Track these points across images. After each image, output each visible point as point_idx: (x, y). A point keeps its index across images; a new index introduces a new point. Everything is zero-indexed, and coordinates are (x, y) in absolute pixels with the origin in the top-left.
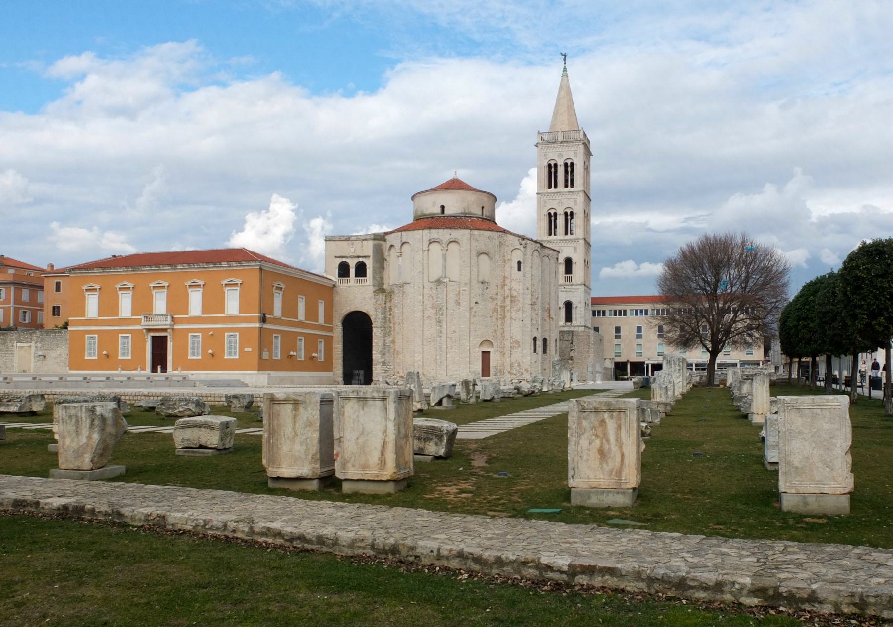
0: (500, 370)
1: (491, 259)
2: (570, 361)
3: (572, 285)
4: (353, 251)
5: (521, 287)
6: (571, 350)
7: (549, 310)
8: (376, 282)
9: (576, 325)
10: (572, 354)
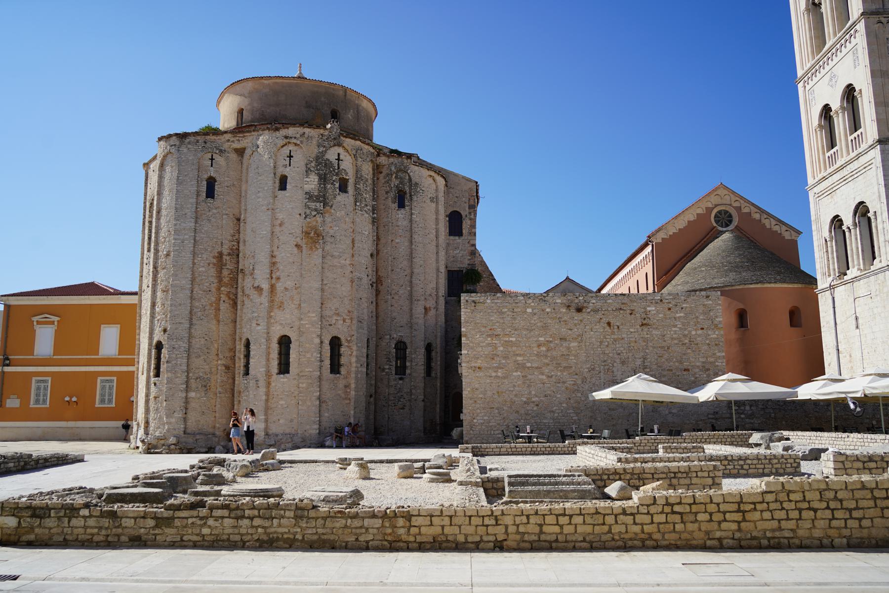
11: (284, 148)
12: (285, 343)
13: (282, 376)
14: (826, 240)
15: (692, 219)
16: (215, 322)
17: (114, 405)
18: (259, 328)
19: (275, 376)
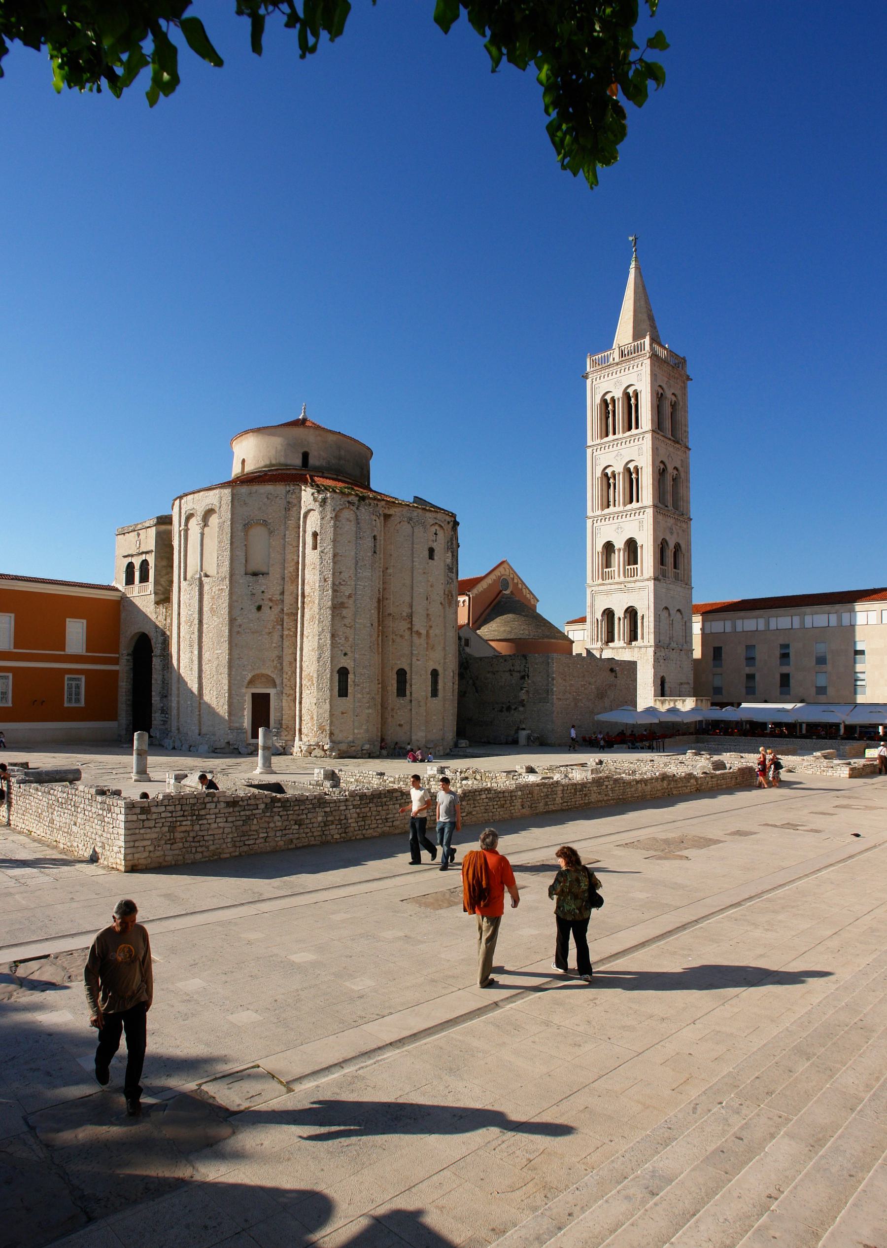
0: (288, 727)
1: (271, 532)
2: (521, 709)
3: (635, 582)
4: (138, 546)
5: (317, 577)
6: (522, 689)
7: (410, 616)
8: (160, 588)
9: (642, 644)
10: (523, 695)
11: (433, 526)
12: (435, 674)
13: (434, 698)
14: (597, 620)
15: (491, 582)
16: (376, 653)
17: (10, 705)
18: (418, 663)
19: (430, 698)
